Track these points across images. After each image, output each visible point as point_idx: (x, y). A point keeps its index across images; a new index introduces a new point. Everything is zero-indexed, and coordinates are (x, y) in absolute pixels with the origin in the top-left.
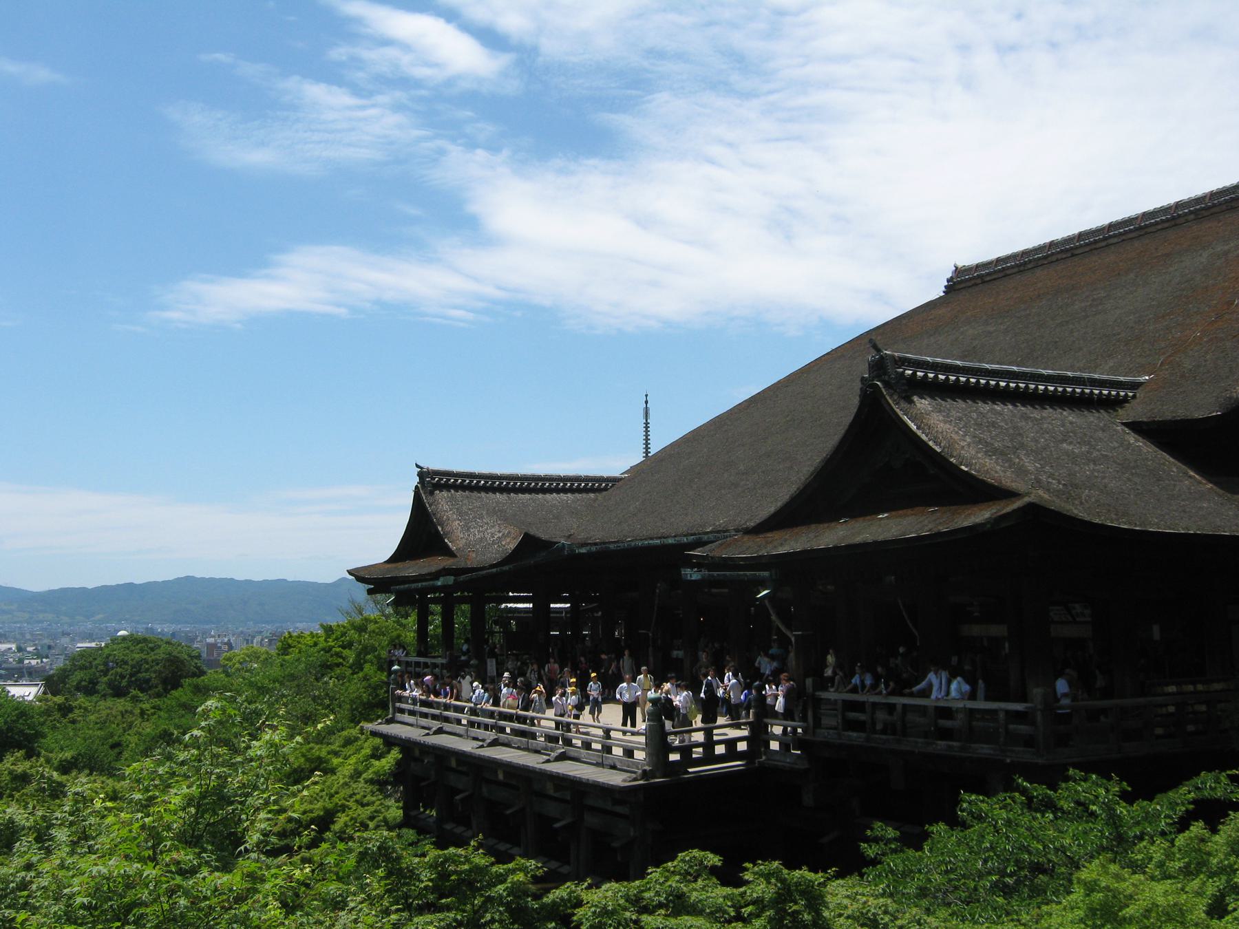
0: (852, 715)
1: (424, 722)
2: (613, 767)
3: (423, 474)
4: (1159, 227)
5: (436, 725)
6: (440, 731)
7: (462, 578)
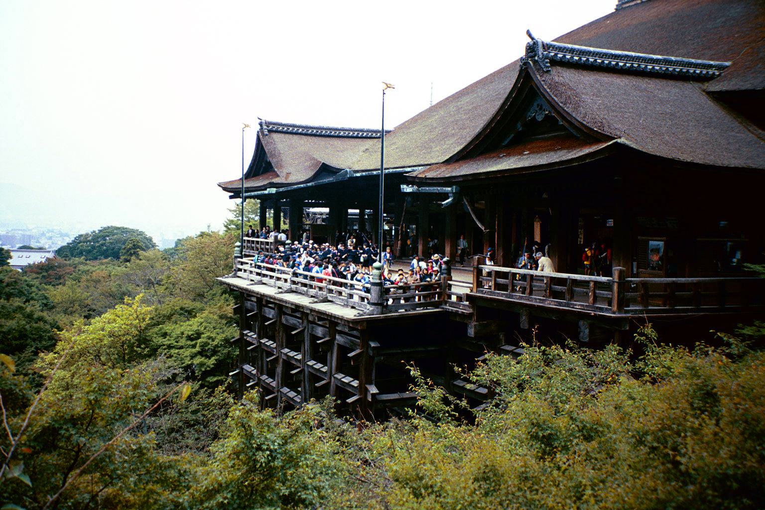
2: (353, 307)
7: (281, 190)
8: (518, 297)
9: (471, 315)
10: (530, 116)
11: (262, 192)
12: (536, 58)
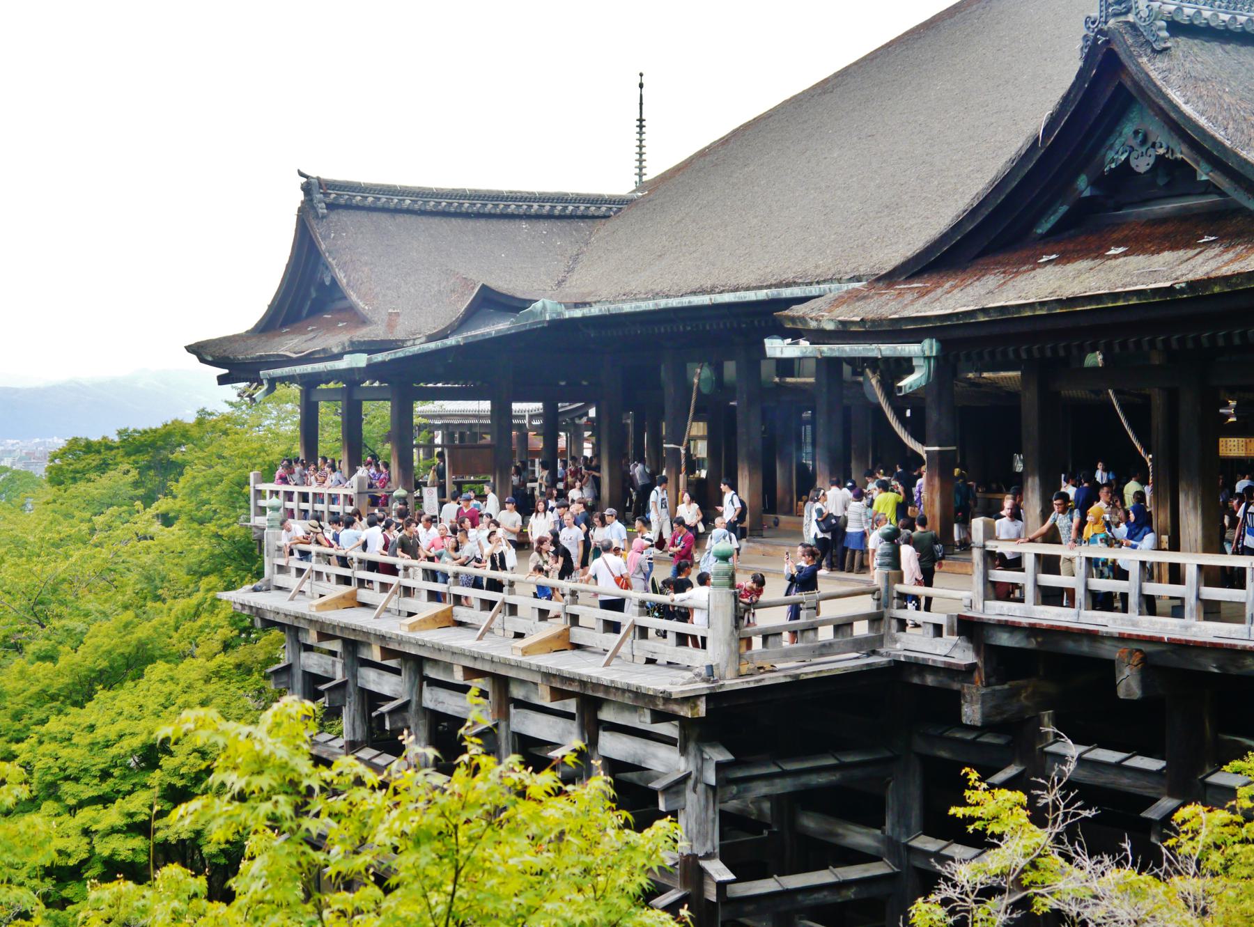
0: (1049, 580)
2: (650, 661)
3: (310, 187)
7: (379, 357)
9: (971, 668)
10: (1113, 160)
12: (1131, 18)
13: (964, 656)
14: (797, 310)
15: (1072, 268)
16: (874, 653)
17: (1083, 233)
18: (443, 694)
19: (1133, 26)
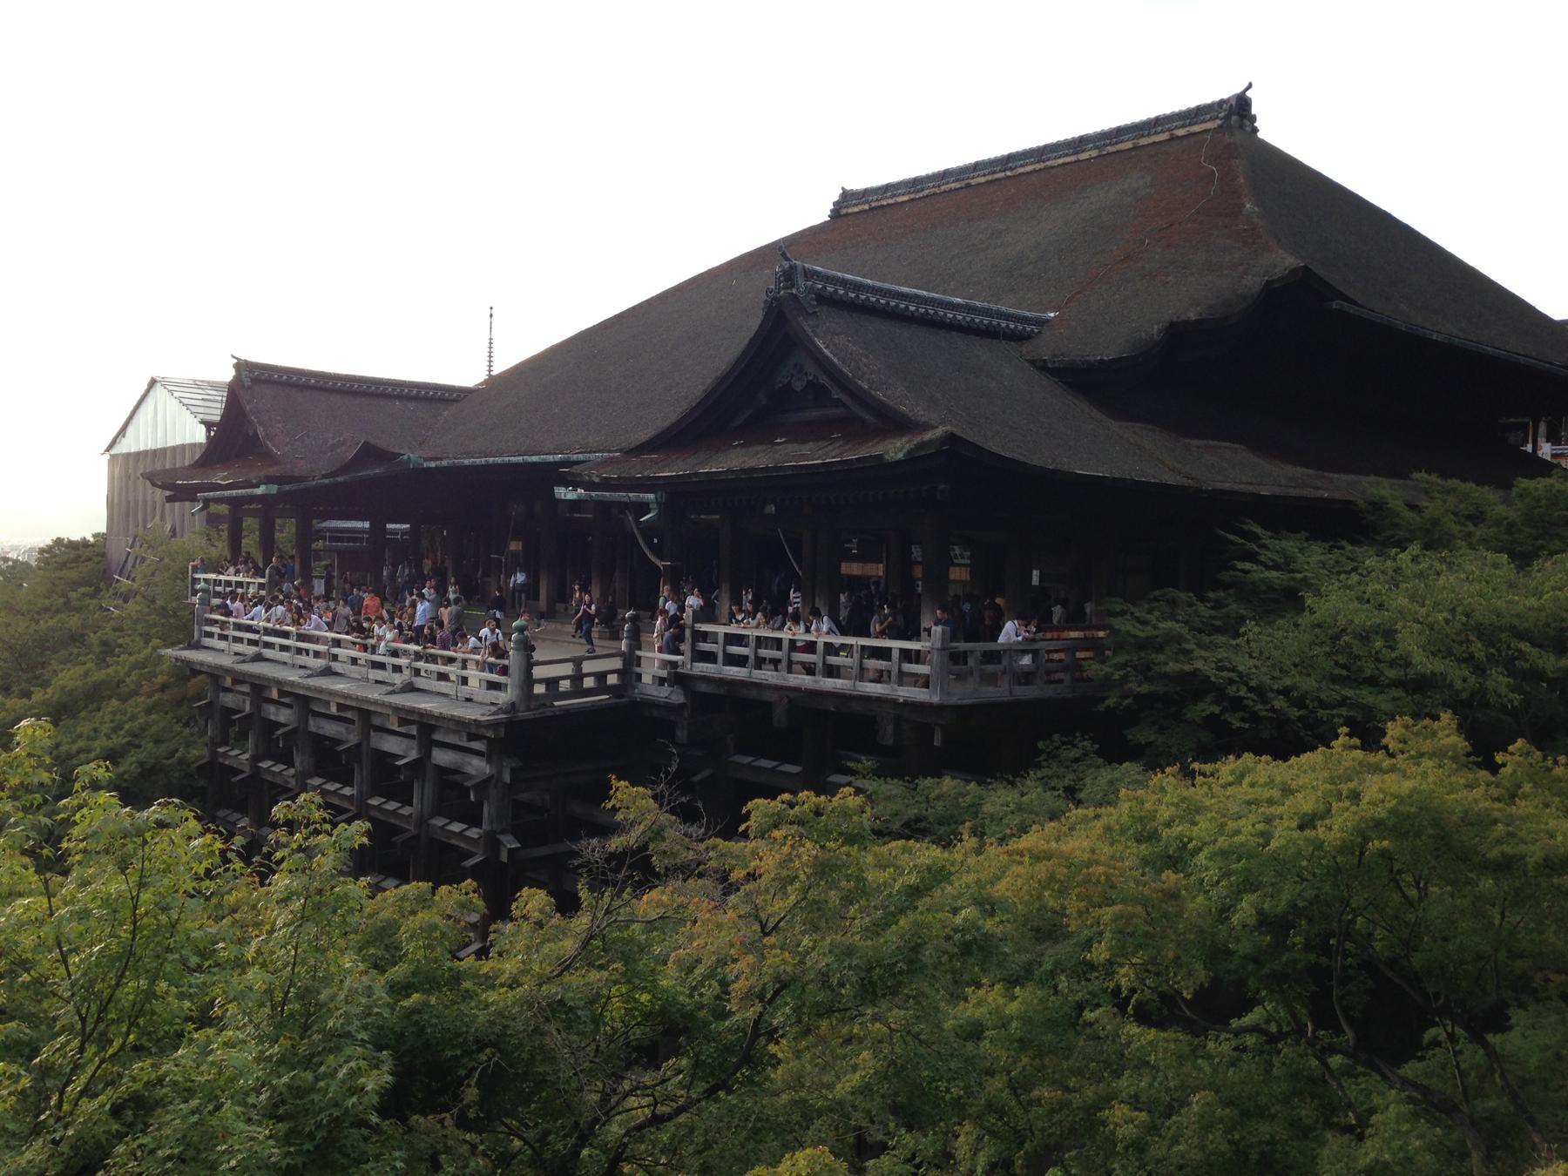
0: (735, 650)
1: (238, 647)
2: (468, 700)
3: (242, 367)
4: (1061, 161)
5: (252, 650)
6: (258, 658)
7: (287, 487)
8: (767, 675)
9: (682, 706)
11: (249, 491)
13: (678, 697)
14: (576, 469)
15: (751, 450)
16: (621, 697)
17: (759, 429)
18: (323, 723)
19: (795, 297)
